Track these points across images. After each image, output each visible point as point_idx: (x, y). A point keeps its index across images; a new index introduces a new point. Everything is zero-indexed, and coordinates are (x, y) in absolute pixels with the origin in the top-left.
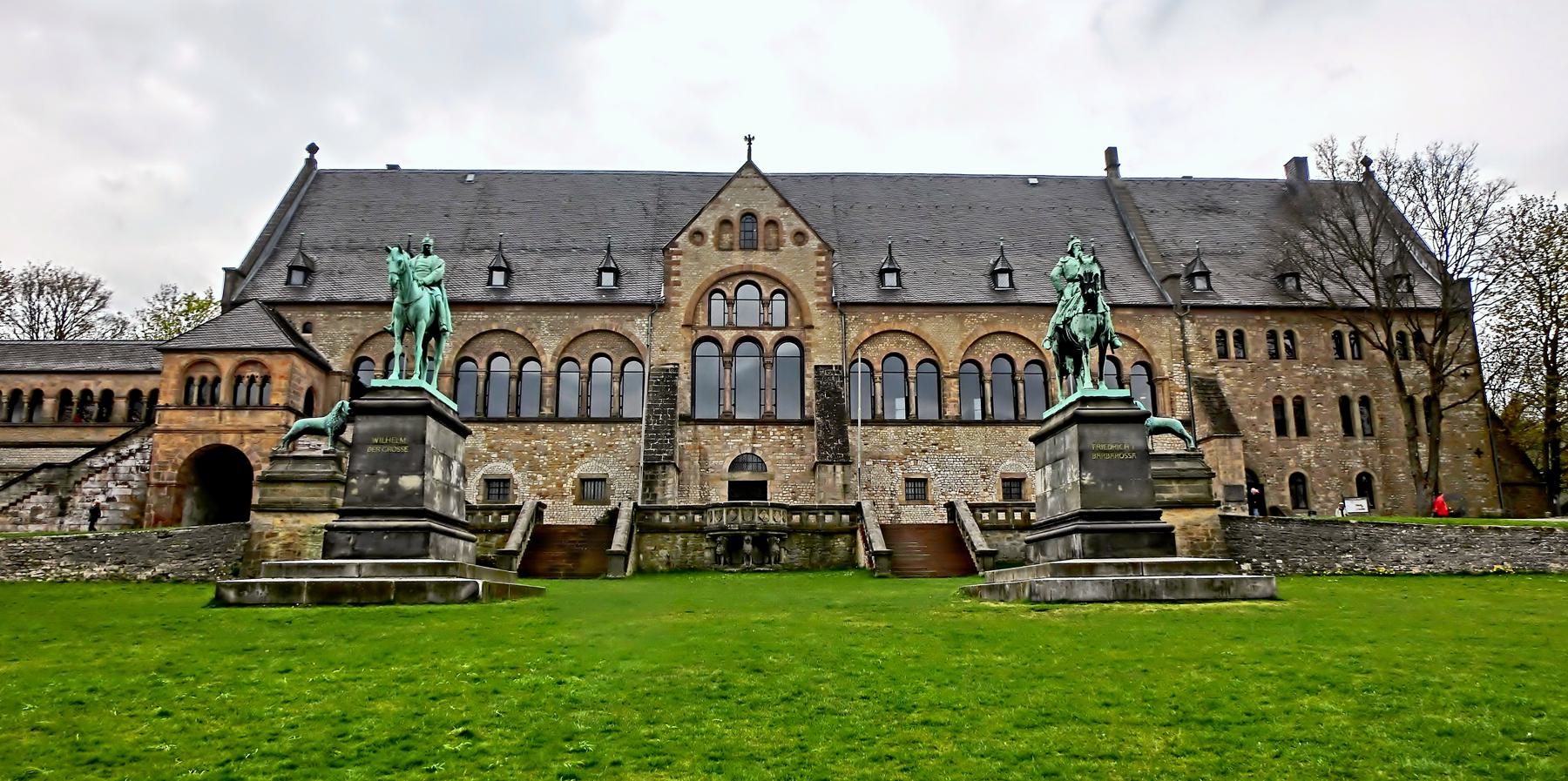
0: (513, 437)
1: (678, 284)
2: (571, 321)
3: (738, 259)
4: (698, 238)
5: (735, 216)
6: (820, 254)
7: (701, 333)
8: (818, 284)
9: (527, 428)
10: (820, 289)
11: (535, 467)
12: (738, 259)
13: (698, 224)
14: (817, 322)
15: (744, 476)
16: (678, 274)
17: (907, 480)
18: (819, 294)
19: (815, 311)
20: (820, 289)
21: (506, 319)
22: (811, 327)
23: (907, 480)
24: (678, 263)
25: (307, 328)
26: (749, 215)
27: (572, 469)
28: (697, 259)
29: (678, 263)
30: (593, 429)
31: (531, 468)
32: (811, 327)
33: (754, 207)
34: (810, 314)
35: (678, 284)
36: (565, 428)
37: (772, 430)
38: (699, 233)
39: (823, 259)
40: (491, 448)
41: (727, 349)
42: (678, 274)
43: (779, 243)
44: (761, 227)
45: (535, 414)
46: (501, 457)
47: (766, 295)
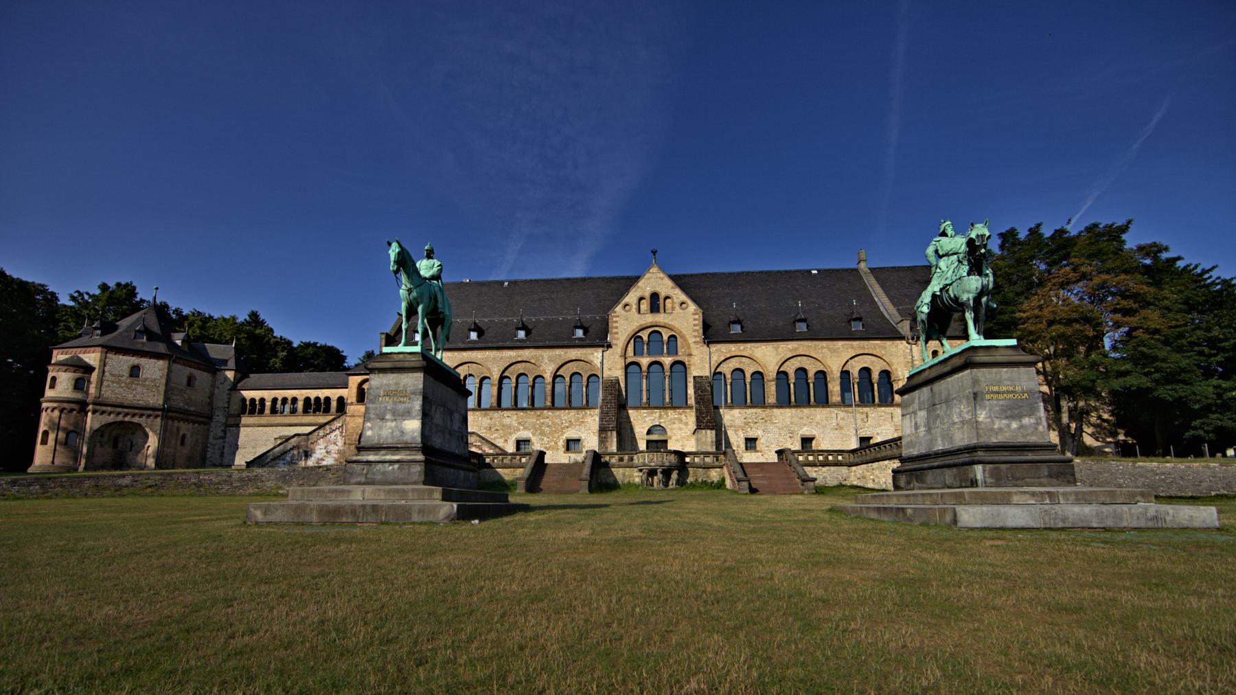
0: (531, 417)
3: (650, 319)
5: (647, 295)
7: (629, 360)
9: (538, 412)
11: (543, 434)
12: (650, 319)
13: (626, 300)
14: (694, 352)
15: (654, 437)
17: (747, 439)
19: (693, 346)
21: (526, 354)
22: (690, 355)
23: (747, 439)
26: (655, 296)
27: (563, 433)
30: (573, 413)
32: (690, 355)
33: (657, 289)
36: (558, 413)
37: (670, 412)
38: (626, 305)
41: (644, 368)
43: (673, 308)
44: (661, 301)
45: (542, 405)
46: (525, 428)
47: (665, 338)
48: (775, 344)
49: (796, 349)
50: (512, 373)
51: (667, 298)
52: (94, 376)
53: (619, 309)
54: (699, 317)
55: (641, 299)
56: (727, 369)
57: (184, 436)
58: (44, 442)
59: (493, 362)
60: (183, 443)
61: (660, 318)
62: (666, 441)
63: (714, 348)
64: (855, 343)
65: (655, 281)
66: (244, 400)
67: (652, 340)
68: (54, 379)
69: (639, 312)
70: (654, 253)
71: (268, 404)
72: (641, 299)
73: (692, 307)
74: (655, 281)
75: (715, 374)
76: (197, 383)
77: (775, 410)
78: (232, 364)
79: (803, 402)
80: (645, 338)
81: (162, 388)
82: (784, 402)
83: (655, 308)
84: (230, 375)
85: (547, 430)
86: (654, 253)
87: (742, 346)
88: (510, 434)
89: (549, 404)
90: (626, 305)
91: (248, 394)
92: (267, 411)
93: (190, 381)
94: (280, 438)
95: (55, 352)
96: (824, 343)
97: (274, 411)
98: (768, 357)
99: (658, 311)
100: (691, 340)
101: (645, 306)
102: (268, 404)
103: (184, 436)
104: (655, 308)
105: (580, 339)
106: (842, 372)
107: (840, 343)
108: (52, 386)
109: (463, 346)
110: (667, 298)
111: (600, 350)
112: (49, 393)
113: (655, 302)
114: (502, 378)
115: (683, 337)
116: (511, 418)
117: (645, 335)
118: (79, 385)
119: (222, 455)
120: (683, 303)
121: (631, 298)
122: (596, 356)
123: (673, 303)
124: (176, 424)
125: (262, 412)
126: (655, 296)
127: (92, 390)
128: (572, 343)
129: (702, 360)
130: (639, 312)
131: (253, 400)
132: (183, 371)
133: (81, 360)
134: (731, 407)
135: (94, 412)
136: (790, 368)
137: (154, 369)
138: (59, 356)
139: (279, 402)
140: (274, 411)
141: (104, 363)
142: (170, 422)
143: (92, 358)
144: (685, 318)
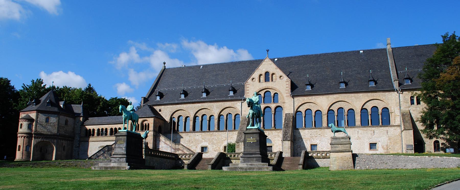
0: (207, 135)
1: (248, 93)
2: (221, 105)
3: (264, 85)
4: (254, 80)
5: (263, 73)
6: (287, 82)
8: (286, 90)
9: (211, 133)
10: (287, 92)
11: (213, 144)
12: (264, 85)
13: (253, 76)
14: (286, 101)
16: (248, 90)
18: (287, 93)
19: (285, 98)
20: (287, 92)
22: (284, 103)
24: (248, 87)
25: (160, 111)
26: (267, 73)
27: (222, 143)
28: (253, 86)
29: (248, 87)
31: (212, 144)
33: (268, 70)
34: (284, 99)
35: (248, 93)
36: (220, 133)
38: (253, 79)
39: (288, 83)
40: (203, 139)
42: (248, 90)
43: (276, 79)
44: (270, 76)
47: (272, 94)
48: (327, 96)
49: (338, 98)
50: (200, 115)
51: (273, 74)
52: (34, 123)
53: (250, 81)
54: (289, 83)
55: (261, 75)
56: (303, 109)
57: (64, 146)
58: (19, 150)
59: (190, 110)
60: (64, 150)
61: (269, 84)
62: (271, 146)
63: (296, 99)
64: (369, 94)
65: (268, 66)
66: (87, 129)
67: (266, 95)
68: (21, 125)
69: (260, 81)
70: (268, 51)
71: (96, 131)
72: (261, 75)
73: (285, 78)
74: (268, 66)
75: (297, 112)
76: (69, 123)
77: (326, 130)
78: (82, 115)
79: (375, 123)
80: (263, 95)
81: (56, 126)
82: (364, 123)
83: (267, 80)
84: (81, 119)
85: (215, 142)
86: (268, 51)
87: (310, 98)
88: (198, 144)
89: (216, 129)
90: (253, 79)
91: (88, 127)
92: (96, 135)
93: (66, 122)
94: (101, 147)
95: (21, 113)
96: (353, 95)
97: (98, 134)
98: (322, 103)
99: (269, 81)
100: (285, 95)
101: (262, 78)
102: (96, 131)
103: (64, 146)
104: (267, 80)
105: (231, 96)
106: (362, 109)
107: (361, 95)
108: (21, 128)
109: (176, 102)
110: (273, 74)
111: (240, 102)
112: (20, 130)
113: (267, 77)
114: (195, 117)
115: (281, 93)
116: (198, 136)
117: (262, 93)
118: (30, 127)
119: (78, 154)
120: (281, 77)
121: (256, 75)
122: (238, 105)
123: (276, 76)
124: (62, 141)
125: (106, 134)
126: (267, 73)
127: (34, 129)
128: (227, 99)
129: (289, 105)
130: (260, 81)
131: (90, 130)
132: (63, 118)
133: (29, 116)
134: (304, 129)
135: (35, 138)
136: (335, 108)
137: (53, 120)
138: (22, 115)
139: (104, 130)
140: (98, 134)
141: (37, 117)
142: (59, 141)
143: (33, 115)
144: (281, 84)
